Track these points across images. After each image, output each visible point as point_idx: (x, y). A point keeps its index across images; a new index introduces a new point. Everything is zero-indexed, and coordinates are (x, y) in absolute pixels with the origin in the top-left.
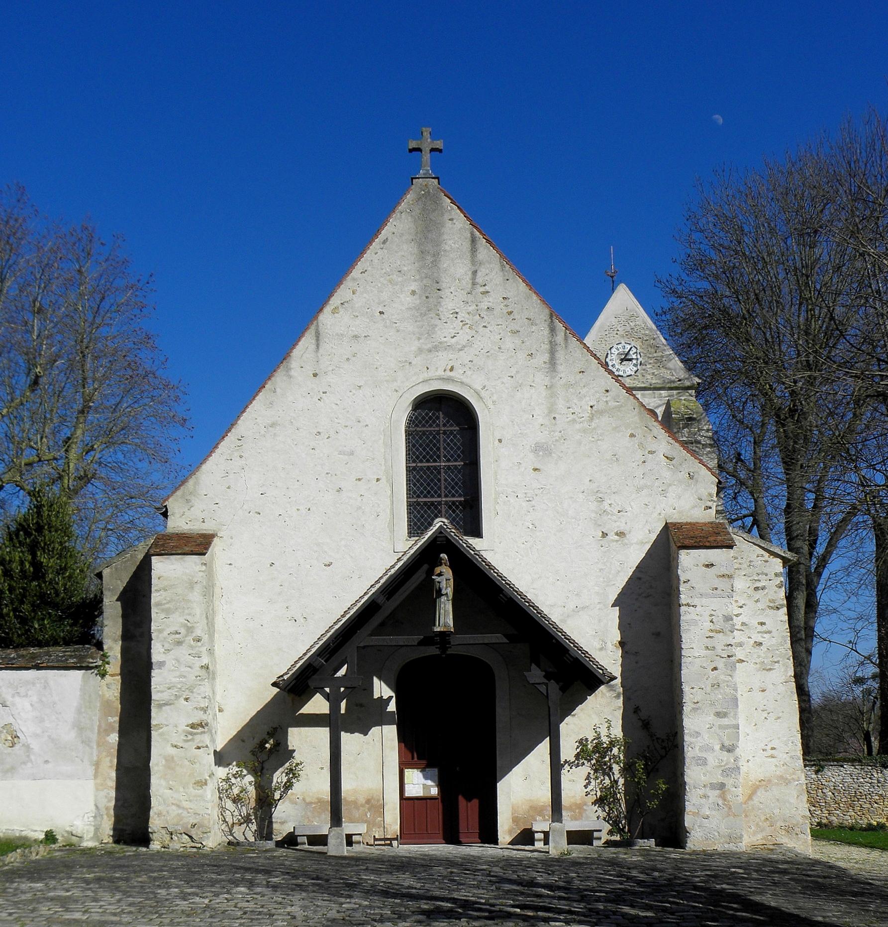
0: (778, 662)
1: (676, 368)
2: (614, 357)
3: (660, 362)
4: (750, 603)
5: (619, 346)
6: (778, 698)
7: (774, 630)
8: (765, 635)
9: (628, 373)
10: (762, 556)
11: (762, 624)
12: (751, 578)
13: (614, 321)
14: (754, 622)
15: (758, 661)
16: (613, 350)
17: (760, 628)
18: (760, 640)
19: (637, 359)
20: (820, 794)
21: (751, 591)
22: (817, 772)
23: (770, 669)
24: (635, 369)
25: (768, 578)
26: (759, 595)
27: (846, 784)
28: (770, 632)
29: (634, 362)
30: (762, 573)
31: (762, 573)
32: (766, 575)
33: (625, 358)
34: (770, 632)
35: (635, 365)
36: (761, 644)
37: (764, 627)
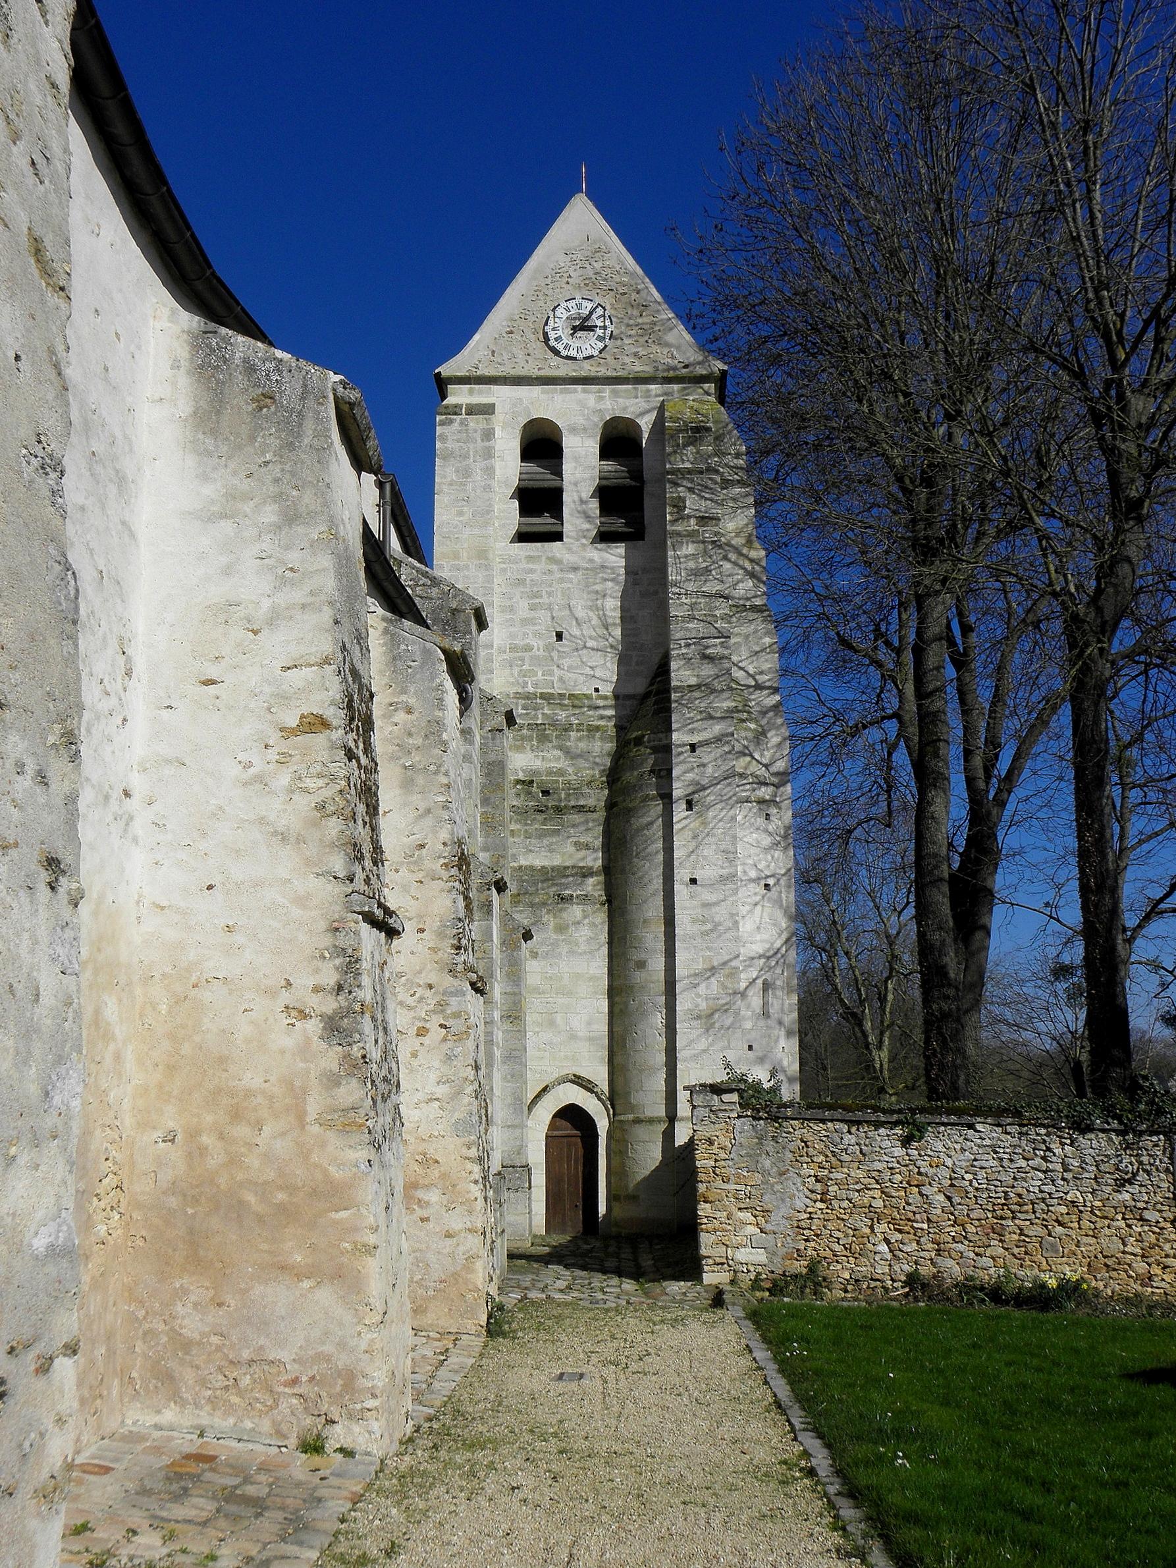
1: (679, 345)
2: (559, 323)
3: (650, 333)
5: (571, 304)
9: (586, 354)
13: (563, 260)
19: (605, 328)
20: (914, 1197)
22: (906, 1142)
24: (601, 345)
27: (982, 1174)
29: (599, 332)
33: (582, 326)
35: (601, 339)
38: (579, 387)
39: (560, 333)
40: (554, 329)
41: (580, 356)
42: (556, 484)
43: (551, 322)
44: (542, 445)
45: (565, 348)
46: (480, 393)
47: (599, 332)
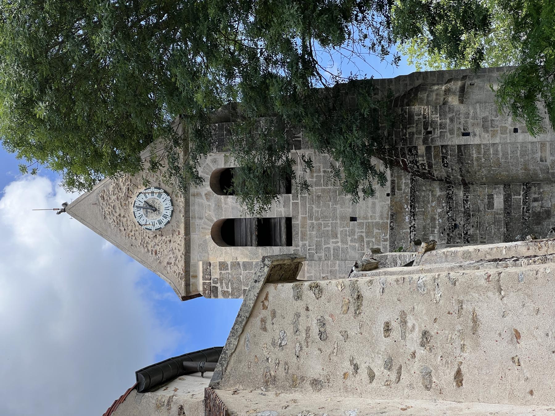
0: (461, 303)
4: (350, 349)
6: (531, 306)
7: (400, 307)
8: (410, 325)
10: (263, 321)
11: (387, 329)
12: (304, 344)
14: (384, 343)
15: (458, 343)
16: (143, 223)
17: (395, 334)
18: (416, 335)
21: (328, 349)
23: (475, 320)
24: (164, 195)
25: (303, 312)
26: (335, 334)
28: (403, 315)
30: (295, 323)
31: (295, 323)
32: (298, 315)
34: (403, 315)
35: (160, 195)
36: (425, 334)
37: (394, 325)
38: (191, 208)
39: (156, 221)
40: (154, 225)
41: (171, 208)
42: (254, 223)
43: (148, 227)
44: (227, 233)
45: (166, 218)
46: (196, 271)
47: (155, 196)
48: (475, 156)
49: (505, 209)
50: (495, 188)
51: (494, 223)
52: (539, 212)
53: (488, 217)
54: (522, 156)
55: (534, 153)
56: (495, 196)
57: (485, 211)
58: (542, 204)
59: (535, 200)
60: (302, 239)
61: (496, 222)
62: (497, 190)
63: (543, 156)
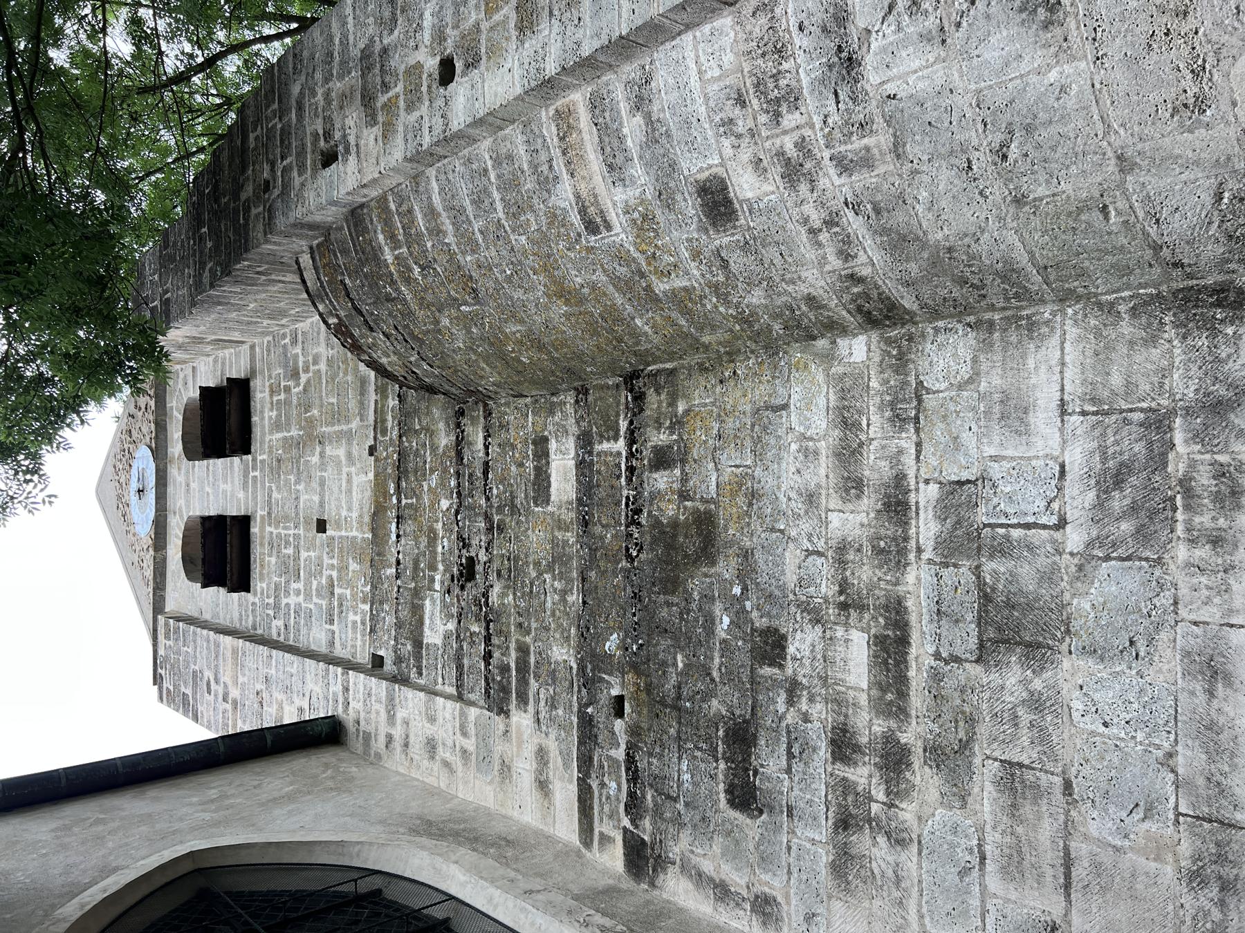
48: (389, 258)
49: (579, 500)
50: (551, 412)
51: (550, 568)
52: (675, 524)
53: (536, 540)
54: (516, 210)
55: (547, 183)
56: (553, 445)
57: (528, 510)
58: (685, 479)
59: (662, 460)
60: (262, 580)
61: (559, 559)
62: (558, 417)
63: (583, 189)
